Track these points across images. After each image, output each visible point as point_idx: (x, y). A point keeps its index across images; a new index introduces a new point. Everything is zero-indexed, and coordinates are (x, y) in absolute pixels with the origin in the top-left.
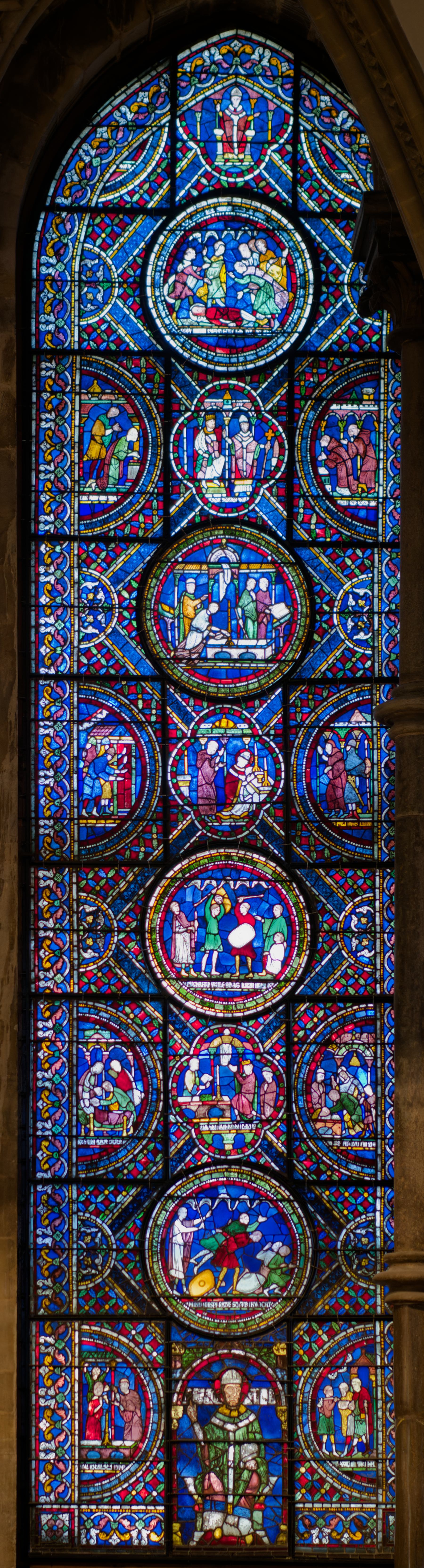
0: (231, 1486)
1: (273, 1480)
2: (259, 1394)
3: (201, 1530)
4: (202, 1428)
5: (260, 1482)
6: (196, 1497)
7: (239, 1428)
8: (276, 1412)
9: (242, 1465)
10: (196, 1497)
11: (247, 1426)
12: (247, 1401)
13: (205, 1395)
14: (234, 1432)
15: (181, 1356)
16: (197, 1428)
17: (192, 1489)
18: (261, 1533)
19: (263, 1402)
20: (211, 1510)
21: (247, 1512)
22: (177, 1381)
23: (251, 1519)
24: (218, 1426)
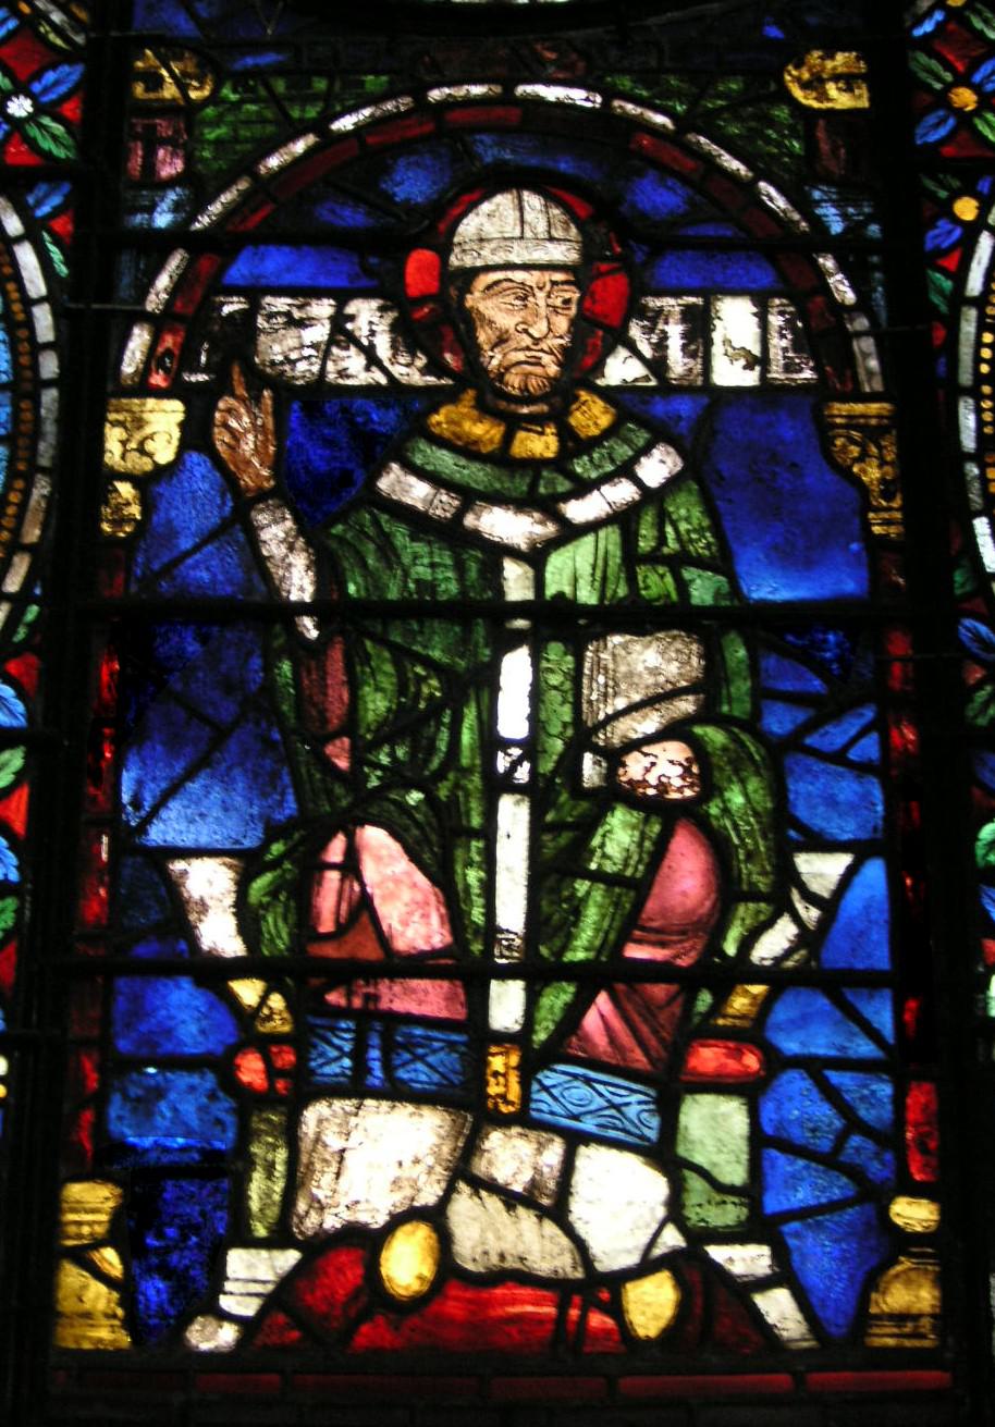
0: (512, 913)
1: (822, 870)
2: (699, 328)
3: (281, 1237)
4: (311, 532)
5: (728, 890)
6: (248, 991)
7: (570, 533)
8: (824, 430)
9: (591, 770)
10: (248, 991)
11: (624, 519)
12: (621, 369)
13: (341, 334)
14: (536, 557)
15: (186, 111)
16: (275, 532)
17: (219, 934)
18: (746, 1260)
19: (730, 374)
20: (356, 1088)
21: (637, 1105)
22: (157, 246)
23: (664, 1154)
24: (418, 521)
